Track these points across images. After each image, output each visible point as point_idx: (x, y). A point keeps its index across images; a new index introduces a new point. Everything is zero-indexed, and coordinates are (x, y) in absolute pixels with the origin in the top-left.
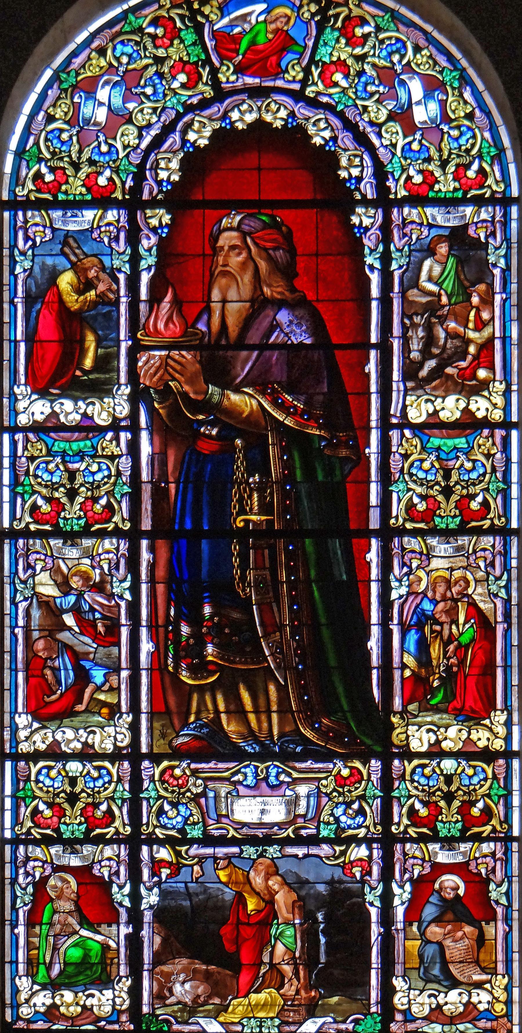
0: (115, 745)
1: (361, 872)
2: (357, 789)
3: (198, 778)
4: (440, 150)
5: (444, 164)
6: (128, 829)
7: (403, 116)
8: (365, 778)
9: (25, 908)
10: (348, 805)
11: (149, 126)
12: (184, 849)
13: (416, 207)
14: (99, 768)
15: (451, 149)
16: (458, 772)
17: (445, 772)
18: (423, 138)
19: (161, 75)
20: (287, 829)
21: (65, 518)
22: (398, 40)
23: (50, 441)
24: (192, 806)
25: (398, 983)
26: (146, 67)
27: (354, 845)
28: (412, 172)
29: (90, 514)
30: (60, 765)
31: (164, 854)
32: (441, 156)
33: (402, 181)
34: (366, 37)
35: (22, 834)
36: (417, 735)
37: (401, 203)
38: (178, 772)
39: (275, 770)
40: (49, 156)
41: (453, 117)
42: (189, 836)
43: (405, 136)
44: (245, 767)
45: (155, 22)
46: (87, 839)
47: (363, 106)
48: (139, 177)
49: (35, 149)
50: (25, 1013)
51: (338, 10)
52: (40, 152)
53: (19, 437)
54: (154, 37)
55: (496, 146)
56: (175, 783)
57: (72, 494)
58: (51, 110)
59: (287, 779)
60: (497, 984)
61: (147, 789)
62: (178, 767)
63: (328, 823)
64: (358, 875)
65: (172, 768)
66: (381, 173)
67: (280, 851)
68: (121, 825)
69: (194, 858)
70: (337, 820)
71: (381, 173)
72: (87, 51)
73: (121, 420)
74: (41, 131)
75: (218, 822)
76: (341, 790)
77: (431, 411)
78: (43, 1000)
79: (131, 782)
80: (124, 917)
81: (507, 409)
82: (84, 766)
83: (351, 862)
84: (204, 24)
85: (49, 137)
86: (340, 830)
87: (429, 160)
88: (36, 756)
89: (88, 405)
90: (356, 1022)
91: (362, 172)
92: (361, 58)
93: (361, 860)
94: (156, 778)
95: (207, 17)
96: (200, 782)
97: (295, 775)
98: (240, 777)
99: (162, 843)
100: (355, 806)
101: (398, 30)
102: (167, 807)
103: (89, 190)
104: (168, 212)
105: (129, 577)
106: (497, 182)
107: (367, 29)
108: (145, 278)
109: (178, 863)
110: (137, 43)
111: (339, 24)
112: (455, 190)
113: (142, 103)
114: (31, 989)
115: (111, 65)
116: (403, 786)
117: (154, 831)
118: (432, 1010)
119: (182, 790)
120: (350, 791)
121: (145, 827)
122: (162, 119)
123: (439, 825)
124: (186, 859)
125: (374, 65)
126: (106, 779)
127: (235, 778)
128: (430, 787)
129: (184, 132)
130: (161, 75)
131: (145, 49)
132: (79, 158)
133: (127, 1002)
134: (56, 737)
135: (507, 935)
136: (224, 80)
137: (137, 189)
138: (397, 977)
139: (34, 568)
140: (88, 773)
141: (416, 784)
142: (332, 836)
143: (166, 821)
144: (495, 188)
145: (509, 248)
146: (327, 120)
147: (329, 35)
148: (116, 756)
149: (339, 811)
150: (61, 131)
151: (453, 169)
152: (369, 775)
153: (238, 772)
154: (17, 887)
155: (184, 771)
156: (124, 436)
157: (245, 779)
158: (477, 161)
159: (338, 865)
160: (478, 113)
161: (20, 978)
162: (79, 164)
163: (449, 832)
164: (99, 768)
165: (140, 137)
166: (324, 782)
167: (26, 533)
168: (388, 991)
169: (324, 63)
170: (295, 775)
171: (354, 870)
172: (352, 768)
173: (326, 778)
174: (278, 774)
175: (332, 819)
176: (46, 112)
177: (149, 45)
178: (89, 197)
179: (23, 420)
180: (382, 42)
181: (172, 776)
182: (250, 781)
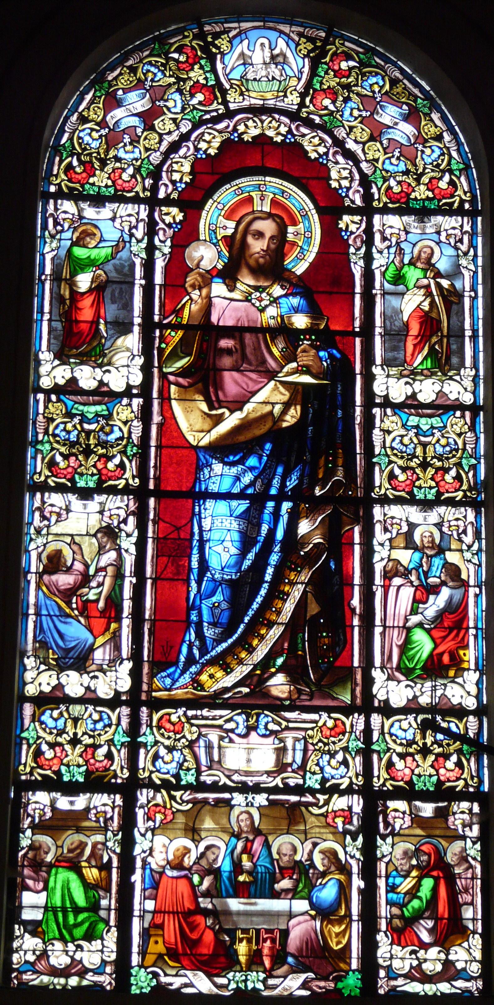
2: (340, 740)
3: (192, 725)
6: (126, 774)
10: (332, 755)
12: (178, 794)
15: (425, 164)
18: (401, 155)
20: (275, 778)
23: (70, 404)
24: (186, 751)
27: (336, 796)
28: (393, 183)
30: (63, 707)
36: (396, 689)
38: (174, 718)
39: (266, 720)
47: (349, 127)
55: (464, 163)
59: (276, 728)
61: (144, 734)
63: (314, 773)
65: (169, 714)
68: (119, 769)
70: (322, 769)
73: (134, 387)
75: (210, 768)
76: (325, 740)
84: (216, 54)
89: (104, 372)
93: (343, 810)
94: (154, 724)
96: (194, 729)
100: (340, 757)
102: (163, 752)
104: (181, 211)
106: (465, 193)
108: (160, 264)
119: (178, 736)
120: (334, 743)
121: (141, 771)
124: (180, 804)
136: (232, 100)
137: (155, 189)
139: (49, 520)
141: (394, 738)
143: (162, 765)
151: (427, 181)
156: (137, 402)
157: (237, 728)
158: (447, 175)
159: (322, 815)
166: (310, 732)
170: (284, 724)
171: (336, 820)
172: (336, 720)
173: (312, 729)
181: (169, 721)
182: (241, 730)
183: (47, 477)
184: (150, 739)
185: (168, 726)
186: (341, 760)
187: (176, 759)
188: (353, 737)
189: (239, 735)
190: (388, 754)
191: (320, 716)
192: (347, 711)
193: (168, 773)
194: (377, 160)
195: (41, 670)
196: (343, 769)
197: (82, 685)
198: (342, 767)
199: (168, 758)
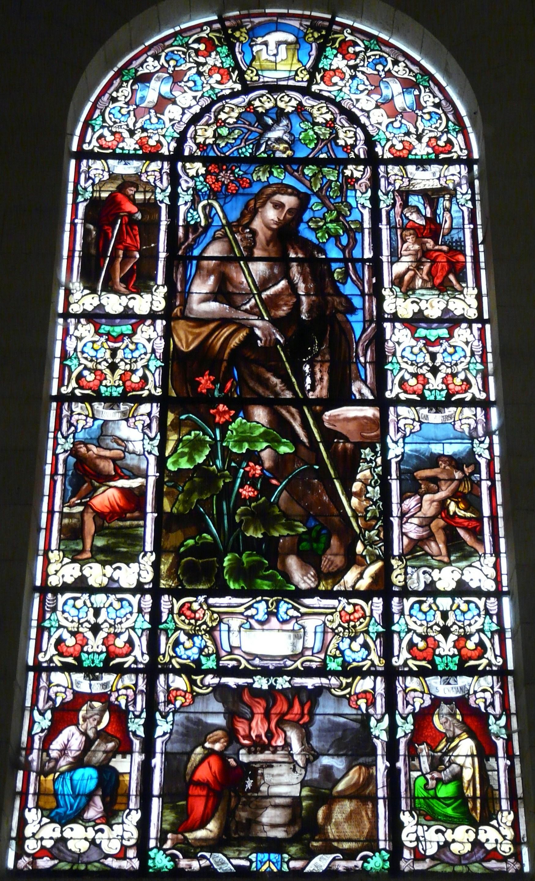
0: (138, 580)
1: (367, 703)
4: (416, 128)
5: (419, 138)
6: (147, 658)
7: (387, 103)
8: (368, 614)
9: (42, 735)
10: (353, 639)
11: (190, 107)
12: (198, 678)
13: (397, 165)
14: (121, 600)
16: (454, 608)
17: (441, 609)
19: (200, 74)
20: (295, 661)
21: (106, 386)
22: (381, 56)
25: (405, 818)
26: (190, 69)
27: (359, 678)
28: (395, 142)
29: (128, 383)
30: (86, 596)
31: (180, 682)
32: (417, 131)
33: (387, 147)
34: (357, 54)
35: (46, 662)
37: (386, 162)
38: (195, 606)
40: (111, 124)
41: (424, 105)
42: (203, 668)
43: (389, 117)
44: (257, 602)
45: (198, 41)
46: (107, 668)
48: (181, 140)
49: (100, 118)
50: (31, 847)
51: (336, 36)
52: (104, 121)
53: (72, 321)
54: (197, 51)
56: (193, 615)
57: (113, 367)
58: (114, 94)
59: (296, 614)
60: (504, 821)
61: (166, 622)
62: (195, 601)
63: (335, 657)
64: (363, 707)
65: (191, 603)
66: (370, 142)
67: (289, 682)
68: (140, 655)
69: (208, 686)
70: (342, 652)
71: (370, 142)
72: (145, 56)
74: (106, 107)
76: (346, 625)
77: (416, 311)
78: (51, 832)
79: (150, 613)
80: (137, 744)
81: (480, 308)
82: (108, 597)
83: (355, 694)
85: (112, 111)
86: (345, 664)
87: (408, 134)
88: (65, 588)
90: (365, 859)
91: (356, 141)
92: (355, 67)
93: (365, 692)
94: (176, 611)
95: (238, 39)
97: (303, 610)
98: (252, 612)
99: (177, 672)
101: (381, 51)
102: (183, 638)
103: (141, 148)
105: (158, 437)
107: (358, 49)
109: (192, 691)
110: (184, 53)
111: (337, 45)
112: (428, 154)
113: (185, 92)
114: (40, 823)
115: (163, 66)
116: (402, 621)
117: (170, 661)
118: (440, 847)
121: (161, 657)
122: (200, 103)
123: (438, 660)
124: (201, 688)
125: (363, 73)
126: (129, 609)
127: (249, 613)
128: (427, 622)
129: (218, 113)
130: (200, 74)
131: (190, 56)
132: (134, 125)
133: (136, 835)
134: (84, 572)
135: (511, 770)
136: (249, 79)
138: (404, 812)
140: (111, 605)
142: (340, 668)
144: (460, 153)
145: (473, 194)
146: (327, 108)
147: (329, 52)
148: (139, 589)
149: (344, 645)
150: (121, 108)
152: (372, 610)
153: (251, 607)
154: (36, 713)
155: (201, 605)
159: (344, 696)
160: (443, 102)
161: (30, 810)
162: (135, 130)
163: (447, 666)
164: (121, 600)
165: (183, 114)
166: (330, 617)
167: (72, 398)
168: (395, 827)
169: (325, 70)
170: (303, 610)
172: (355, 605)
173: (332, 614)
174: (288, 609)
175: (338, 652)
176: (111, 95)
177: (193, 55)
178: (140, 152)
179: (75, 309)
180: (369, 57)
181: (189, 608)
182: (261, 616)
183: (74, 389)
184: (171, 626)
185: (188, 613)
186: (362, 642)
187: (197, 644)
188: (373, 621)
189: (258, 621)
190: (409, 636)
191: (340, 601)
192: (367, 596)
193: (189, 658)
194: (380, 124)
195: (64, 563)
196: (364, 652)
197: (104, 575)
198: (363, 649)
199: (188, 644)
